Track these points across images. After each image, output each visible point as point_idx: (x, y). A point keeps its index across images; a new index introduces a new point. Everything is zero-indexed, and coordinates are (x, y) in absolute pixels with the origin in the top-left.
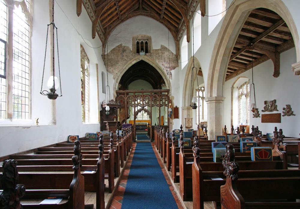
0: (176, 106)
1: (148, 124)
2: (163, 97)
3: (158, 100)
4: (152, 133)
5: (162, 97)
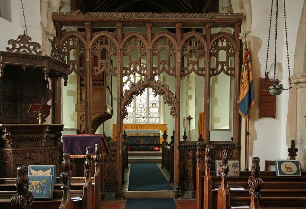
1: (161, 134)
2: (220, 44)
4: (179, 165)
5: (217, 41)
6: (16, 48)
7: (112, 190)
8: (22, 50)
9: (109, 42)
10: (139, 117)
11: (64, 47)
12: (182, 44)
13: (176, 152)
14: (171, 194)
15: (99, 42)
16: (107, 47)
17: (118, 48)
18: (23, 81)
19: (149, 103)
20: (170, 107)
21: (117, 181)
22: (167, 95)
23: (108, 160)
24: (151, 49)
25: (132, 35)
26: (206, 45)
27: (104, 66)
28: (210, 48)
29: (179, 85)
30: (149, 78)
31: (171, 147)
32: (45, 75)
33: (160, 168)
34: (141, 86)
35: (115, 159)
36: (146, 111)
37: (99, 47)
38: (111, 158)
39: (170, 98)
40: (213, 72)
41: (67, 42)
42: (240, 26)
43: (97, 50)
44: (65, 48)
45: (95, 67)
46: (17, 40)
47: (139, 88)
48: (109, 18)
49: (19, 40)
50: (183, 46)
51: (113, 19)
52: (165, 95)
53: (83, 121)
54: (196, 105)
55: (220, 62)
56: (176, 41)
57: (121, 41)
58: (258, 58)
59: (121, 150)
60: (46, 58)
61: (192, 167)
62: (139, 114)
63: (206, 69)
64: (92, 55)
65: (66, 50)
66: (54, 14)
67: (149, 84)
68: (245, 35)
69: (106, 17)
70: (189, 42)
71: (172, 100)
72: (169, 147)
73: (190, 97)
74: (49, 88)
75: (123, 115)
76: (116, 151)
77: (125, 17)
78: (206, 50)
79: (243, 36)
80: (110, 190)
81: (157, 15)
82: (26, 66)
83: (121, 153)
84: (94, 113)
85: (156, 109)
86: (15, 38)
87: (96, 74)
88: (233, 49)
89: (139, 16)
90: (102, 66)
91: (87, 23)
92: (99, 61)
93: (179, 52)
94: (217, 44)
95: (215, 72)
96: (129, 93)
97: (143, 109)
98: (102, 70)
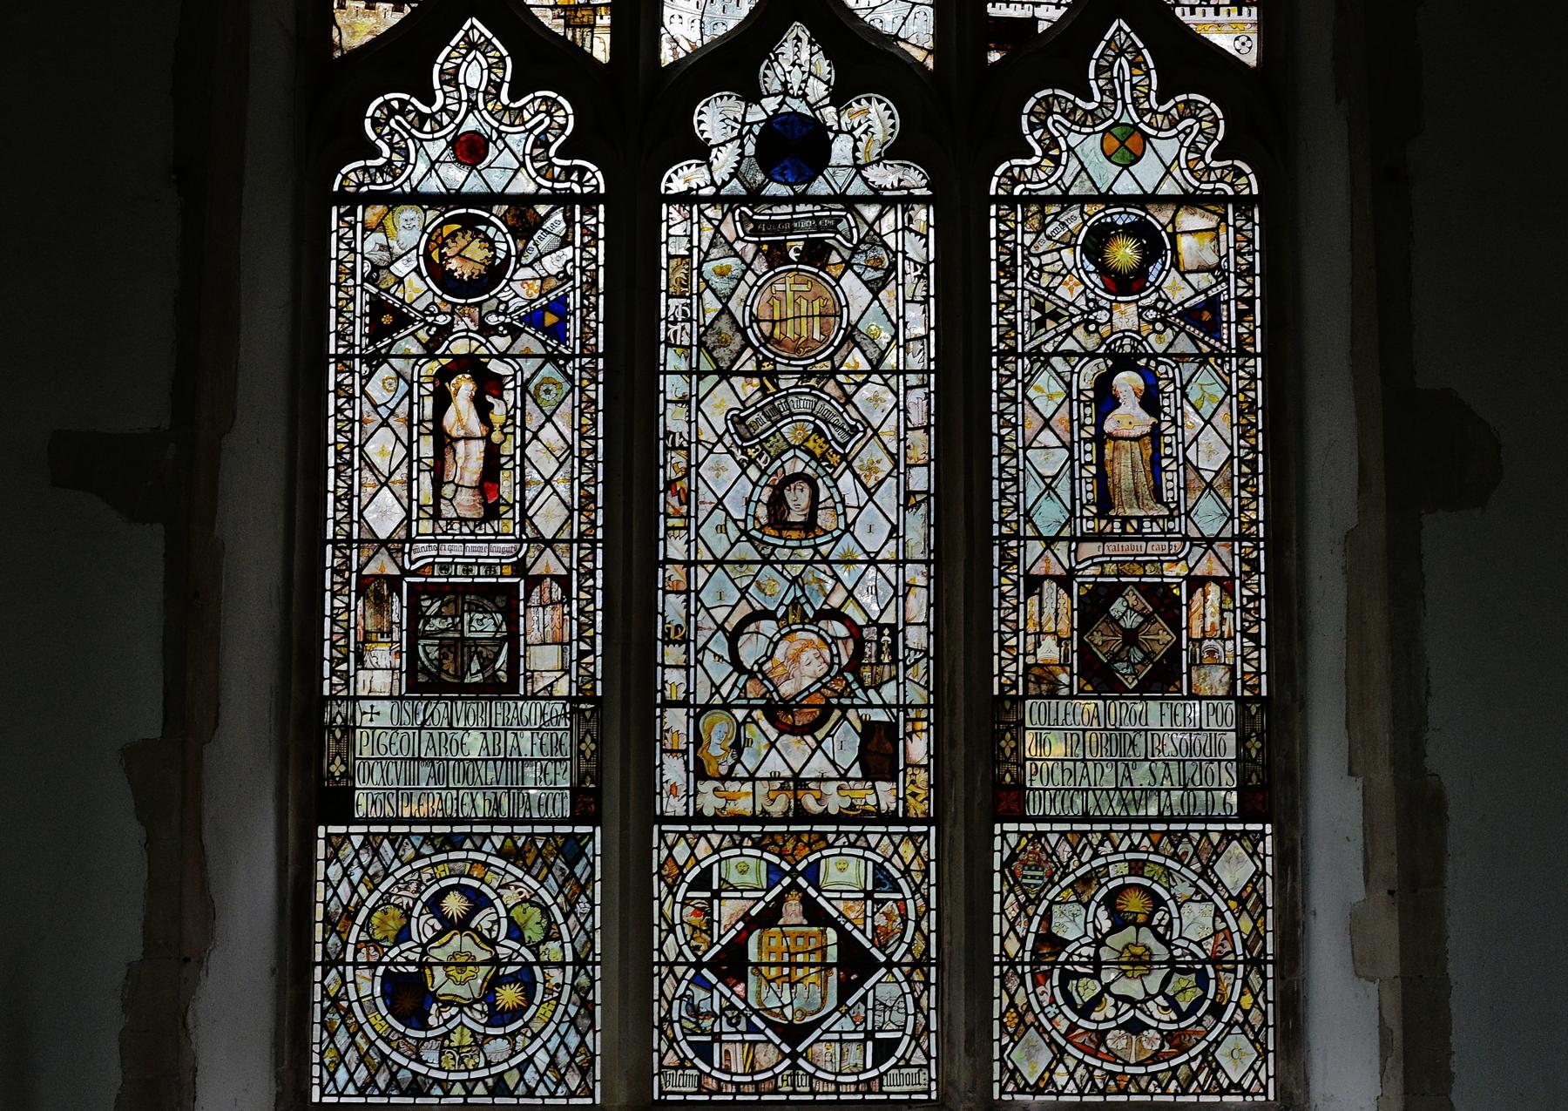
10: (732, 964)
19: (1005, 585)
36: (912, 789)
97: (844, 745)
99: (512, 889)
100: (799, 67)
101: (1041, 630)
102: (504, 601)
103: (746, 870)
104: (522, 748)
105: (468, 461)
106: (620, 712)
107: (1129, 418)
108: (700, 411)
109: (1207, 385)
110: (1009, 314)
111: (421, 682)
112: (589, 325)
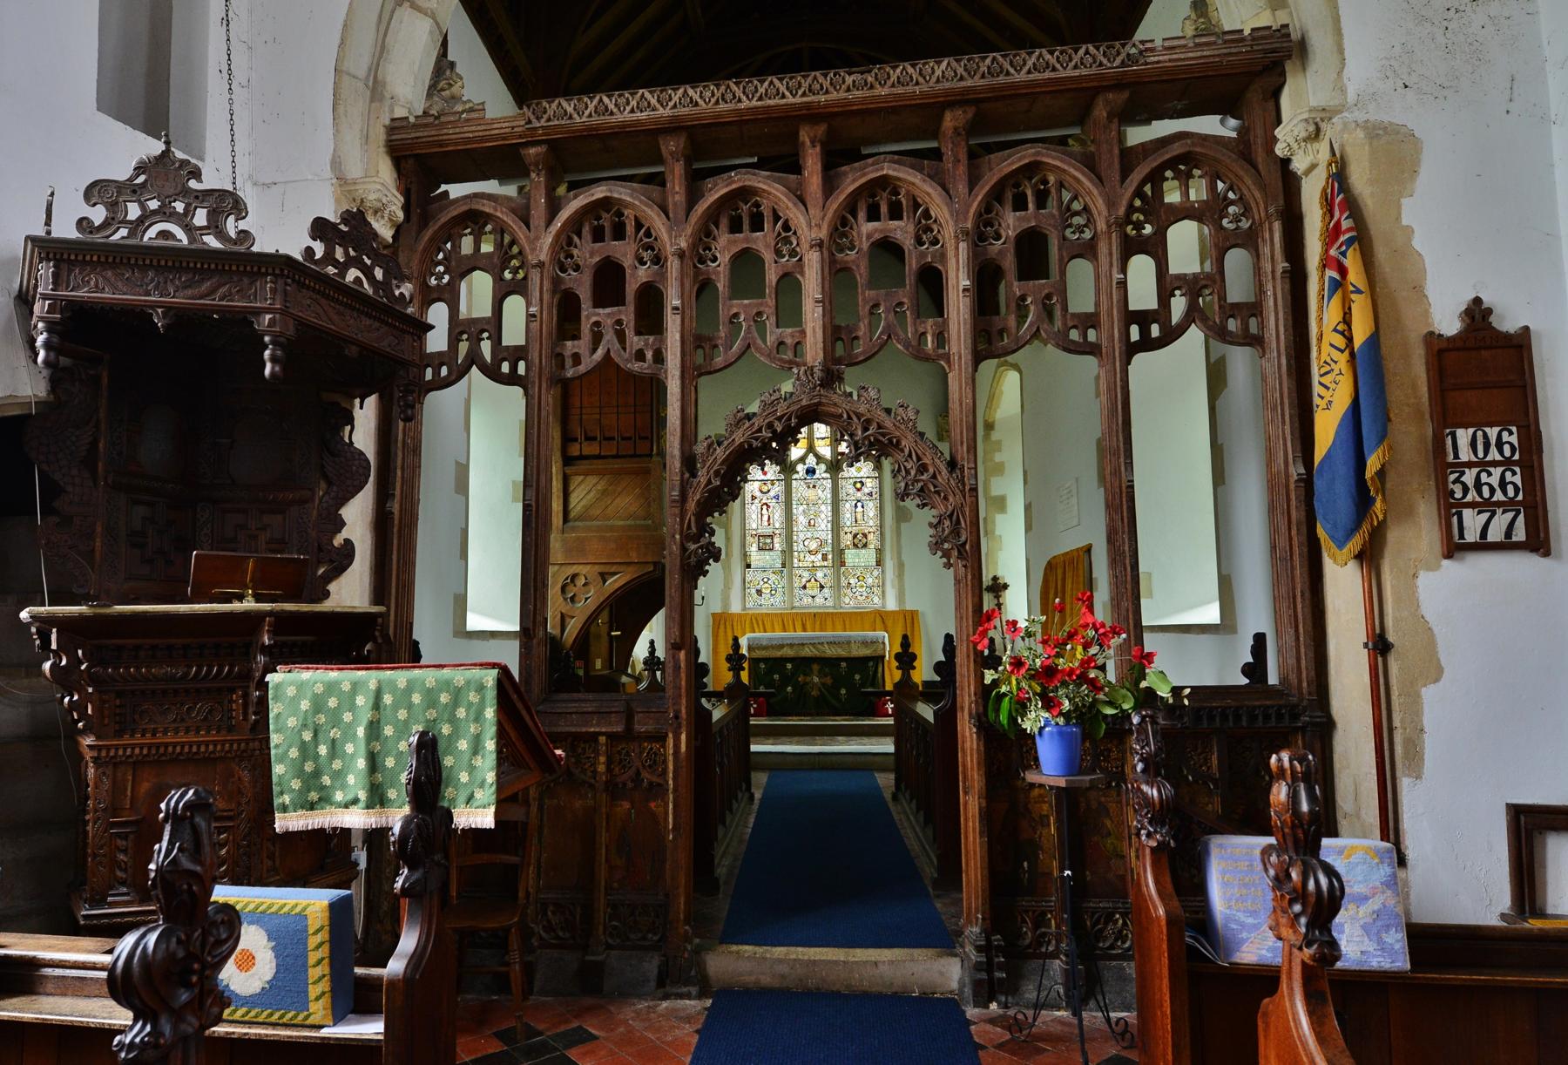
0: (1477, 314)
1: (891, 648)
2: (1173, 197)
3: (1088, 250)
4: (987, 816)
5: (1156, 178)
6: (124, 222)
7: (644, 938)
8: (152, 232)
9: (630, 228)
11: (439, 263)
12: (975, 204)
13: (968, 745)
14: (948, 973)
15: (586, 230)
16: (624, 252)
17: (670, 249)
18: (209, 408)
20: (929, 515)
21: (667, 896)
22: (910, 455)
23: (625, 784)
24: (826, 243)
25: (734, 186)
26: (1100, 203)
27: (609, 336)
28: (1122, 211)
29: (969, 401)
30: (818, 373)
31: (935, 713)
32: (267, 353)
33: (888, 796)
34: (779, 419)
35: (655, 779)
36: (829, 563)
37: (587, 253)
38: (638, 773)
39: (923, 468)
40: (1145, 332)
41: (449, 246)
42: (1276, 94)
43: (577, 268)
44: (441, 268)
45: (569, 343)
46: (131, 179)
47: (770, 426)
48: (626, 116)
49: (141, 179)
50: (981, 215)
51: (643, 116)
52: (900, 457)
53: (572, 599)
54: (1028, 528)
55: (1181, 278)
56: (948, 192)
57: (682, 213)
58: (1409, 231)
59: (683, 737)
60: (279, 265)
61: (1058, 829)
62: (806, 575)
63: (1104, 318)
64: (554, 292)
65: (446, 278)
66: (395, 126)
67: (820, 404)
68: (1312, 128)
69: (612, 113)
70: (1009, 195)
71: (934, 477)
72: (926, 711)
73: (1000, 504)
74: (351, 443)
75: (693, 560)
76: (662, 739)
77: (697, 104)
78: (1101, 225)
79: (1303, 134)
80: (632, 936)
81: (849, 80)
82: (168, 308)
83: (683, 748)
84: (613, 569)
85: (869, 556)
86: (122, 172)
87: (570, 373)
88: (1247, 212)
89: (762, 90)
90: (597, 338)
91: (532, 151)
92: (584, 314)
93: (963, 246)
94: (1159, 193)
95: (1155, 331)
96: (720, 453)
97: (820, 556)
98: (600, 352)
99: (773, 577)
100: (811, 460)
101: (847, 540)
102: (771, 537)
103: (806, 575)
104: (773, 559)
105: (765, 518)
106: (788, 552)
107: (859, 509)
108: (798, 510)
109: (871, 504)
110: (842, 495)
111: (760, 549)
112: (782, 498)
